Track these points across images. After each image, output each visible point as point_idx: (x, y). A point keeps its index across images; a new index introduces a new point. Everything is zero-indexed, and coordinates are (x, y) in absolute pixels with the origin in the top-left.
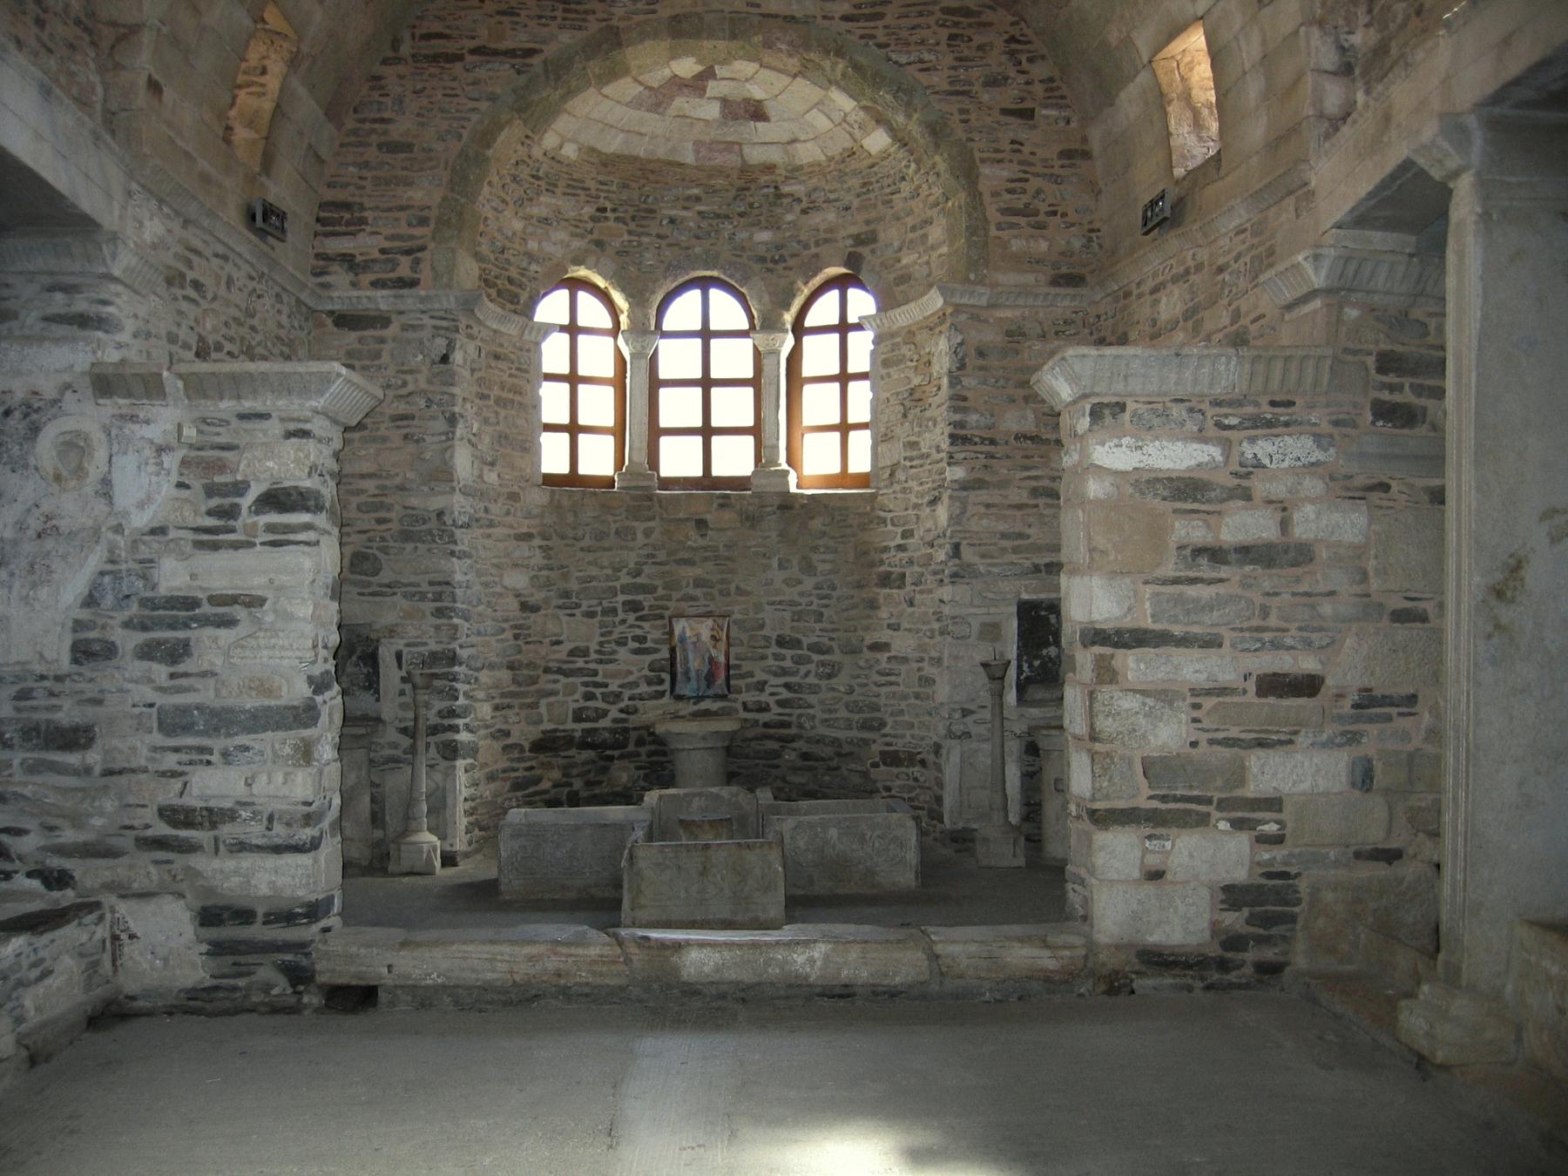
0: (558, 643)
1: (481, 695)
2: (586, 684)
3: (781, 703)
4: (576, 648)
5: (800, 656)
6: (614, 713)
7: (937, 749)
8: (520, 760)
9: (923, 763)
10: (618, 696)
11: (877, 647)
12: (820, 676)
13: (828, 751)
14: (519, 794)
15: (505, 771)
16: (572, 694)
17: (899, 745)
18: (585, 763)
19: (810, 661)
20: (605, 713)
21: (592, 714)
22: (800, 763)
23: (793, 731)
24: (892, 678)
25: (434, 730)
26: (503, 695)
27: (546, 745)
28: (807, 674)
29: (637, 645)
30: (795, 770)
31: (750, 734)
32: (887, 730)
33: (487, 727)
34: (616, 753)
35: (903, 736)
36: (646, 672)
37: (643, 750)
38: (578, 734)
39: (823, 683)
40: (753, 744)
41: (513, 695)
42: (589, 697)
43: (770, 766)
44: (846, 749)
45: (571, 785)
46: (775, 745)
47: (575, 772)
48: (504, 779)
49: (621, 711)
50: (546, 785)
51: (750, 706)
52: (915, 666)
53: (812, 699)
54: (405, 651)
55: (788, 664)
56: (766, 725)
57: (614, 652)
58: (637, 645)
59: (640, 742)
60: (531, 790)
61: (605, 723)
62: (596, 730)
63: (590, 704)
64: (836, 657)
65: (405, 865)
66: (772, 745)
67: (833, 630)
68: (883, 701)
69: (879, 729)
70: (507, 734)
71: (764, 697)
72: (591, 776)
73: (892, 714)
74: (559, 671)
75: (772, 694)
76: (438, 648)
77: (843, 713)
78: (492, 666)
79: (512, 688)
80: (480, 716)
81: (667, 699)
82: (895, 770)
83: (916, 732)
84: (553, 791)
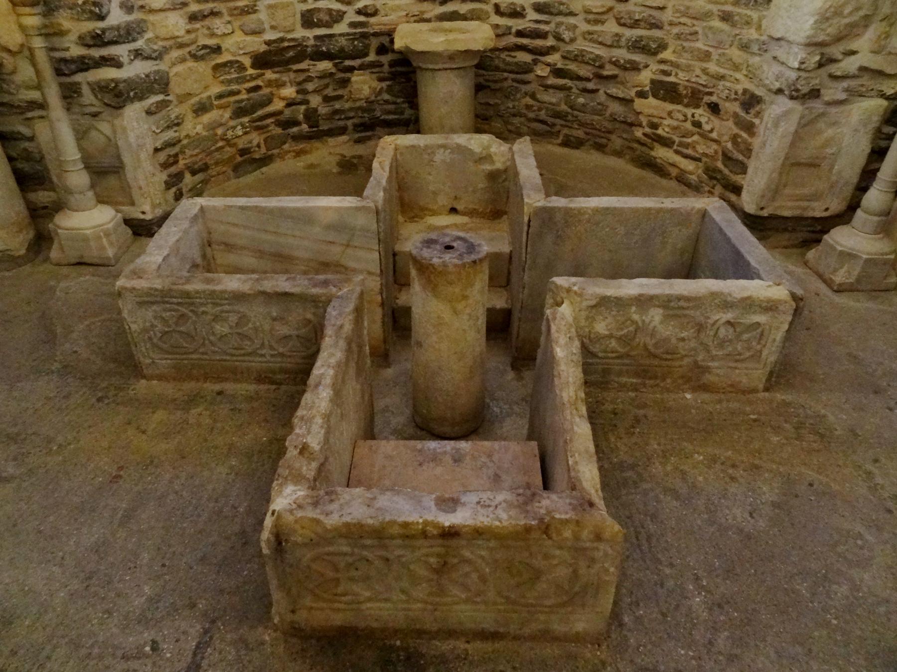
6: (351, 16)
7: (751, 102)
8: (240, 80)
9: (714, 108)
14: (246, 120)
15: (220, 96)
17: (679, 78)
18: (323, 76)
20: (340, 16)
21: (326, 18)
22: (552, 81)
23: (550, 42)
30: (547, 87)
31: (502, 43)
32: (666, 55)
33: (181, 46)
34: (356, 63)
35: (688, 69)
37: (385, 59)
40: (503, 56)
43: (518, 81)
44: (609, 71)
45: (307, 102)
47: (310, 86)
48: (220, 107)
49: (359, 12)
50: (277, 105)
56: (520, 34)
60: (260, 113)
61: (341, 28)
62: (331, 36)
65: (73, 255)
66: (524, 57)
69: (655, 53)
70: (217, 50)
72: (330, 92)
77: (611, 27)
80: (163, 33)
82: (670, 107)
83: (713, 67)
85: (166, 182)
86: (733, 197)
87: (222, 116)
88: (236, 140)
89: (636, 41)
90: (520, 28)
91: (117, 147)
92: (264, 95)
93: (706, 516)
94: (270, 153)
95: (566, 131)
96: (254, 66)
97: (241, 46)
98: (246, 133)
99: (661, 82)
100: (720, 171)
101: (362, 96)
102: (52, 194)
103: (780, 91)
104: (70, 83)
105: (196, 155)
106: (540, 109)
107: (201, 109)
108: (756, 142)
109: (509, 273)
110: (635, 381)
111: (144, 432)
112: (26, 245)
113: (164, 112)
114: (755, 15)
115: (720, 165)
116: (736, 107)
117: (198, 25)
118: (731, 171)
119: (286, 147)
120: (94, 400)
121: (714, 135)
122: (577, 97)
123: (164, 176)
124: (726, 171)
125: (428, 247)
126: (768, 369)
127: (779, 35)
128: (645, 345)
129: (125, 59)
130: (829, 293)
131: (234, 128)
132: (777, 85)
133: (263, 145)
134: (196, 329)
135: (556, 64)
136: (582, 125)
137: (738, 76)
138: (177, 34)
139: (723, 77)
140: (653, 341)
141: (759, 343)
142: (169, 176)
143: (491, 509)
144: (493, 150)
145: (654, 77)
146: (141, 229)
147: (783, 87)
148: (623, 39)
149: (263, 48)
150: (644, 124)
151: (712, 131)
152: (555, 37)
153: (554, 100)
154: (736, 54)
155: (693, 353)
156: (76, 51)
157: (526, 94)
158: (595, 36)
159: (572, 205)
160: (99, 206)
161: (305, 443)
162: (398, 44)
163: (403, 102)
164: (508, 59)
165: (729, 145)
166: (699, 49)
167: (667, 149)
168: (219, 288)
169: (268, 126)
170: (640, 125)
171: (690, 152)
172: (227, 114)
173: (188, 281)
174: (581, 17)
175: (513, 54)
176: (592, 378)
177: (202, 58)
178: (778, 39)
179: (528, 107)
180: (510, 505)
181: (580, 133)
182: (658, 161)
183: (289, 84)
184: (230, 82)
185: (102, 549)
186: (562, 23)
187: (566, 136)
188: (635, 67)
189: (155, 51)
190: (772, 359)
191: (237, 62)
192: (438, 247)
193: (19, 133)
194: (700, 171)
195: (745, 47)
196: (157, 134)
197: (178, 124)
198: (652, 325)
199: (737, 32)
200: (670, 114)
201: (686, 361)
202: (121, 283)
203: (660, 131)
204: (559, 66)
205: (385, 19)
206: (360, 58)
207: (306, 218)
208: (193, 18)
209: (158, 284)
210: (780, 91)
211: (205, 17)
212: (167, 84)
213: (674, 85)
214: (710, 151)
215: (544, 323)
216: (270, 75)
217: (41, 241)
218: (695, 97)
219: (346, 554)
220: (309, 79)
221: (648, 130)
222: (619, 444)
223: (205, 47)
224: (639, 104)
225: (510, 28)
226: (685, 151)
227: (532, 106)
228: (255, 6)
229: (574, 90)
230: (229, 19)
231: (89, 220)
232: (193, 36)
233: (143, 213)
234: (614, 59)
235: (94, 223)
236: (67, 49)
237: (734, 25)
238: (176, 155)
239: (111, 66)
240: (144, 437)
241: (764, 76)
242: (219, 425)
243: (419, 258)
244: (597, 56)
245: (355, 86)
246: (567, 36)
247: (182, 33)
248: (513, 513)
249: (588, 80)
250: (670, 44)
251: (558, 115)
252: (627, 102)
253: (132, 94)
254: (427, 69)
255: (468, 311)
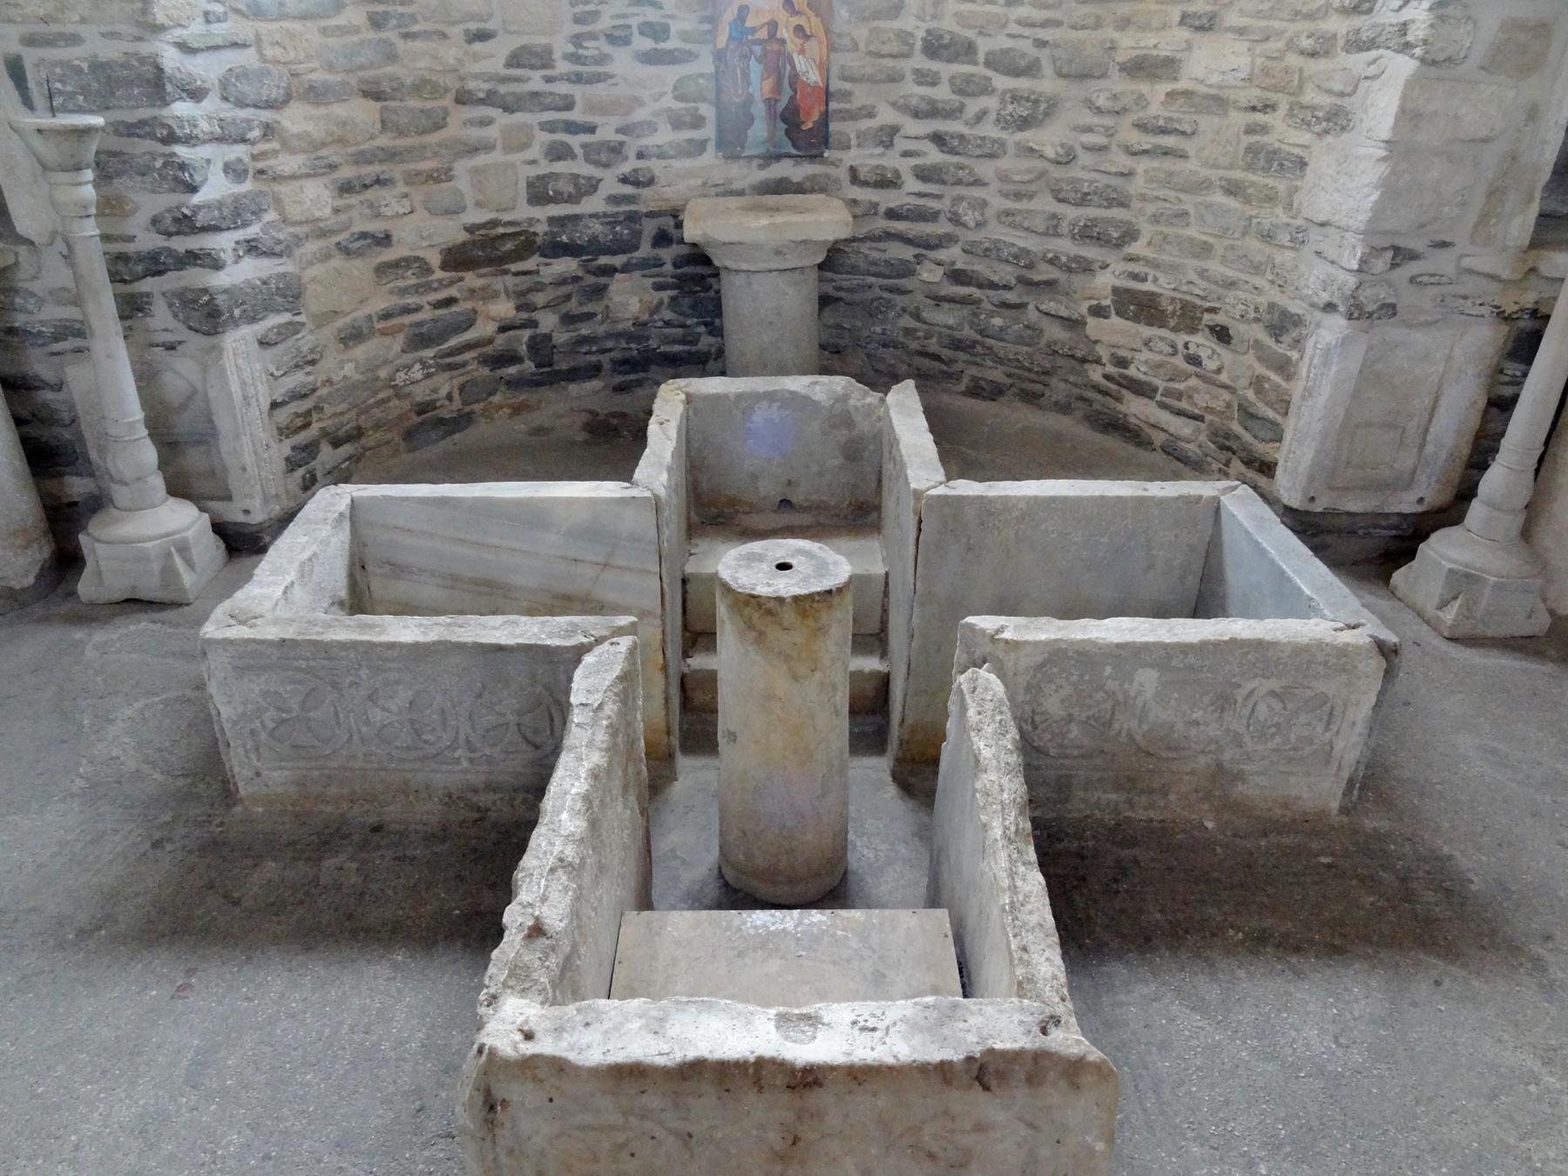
0: (482, 36)
1: (287, 163)
2: (549, 127)
3: (924, 174)
4: (524, 48)
5: (969, 79)
6: (610, 185)
8: (417, 289)
9: (1222, 335)
10: (616, 150)
11: (1141, 67)
12: (1004, 122)
13: (1005, 273)
14: (428, 353)
15: (387, 316)
16: (524, 146)
17: (1160, 285)
18: (562, 281)
19: (986, 89)
20: (593, 186)
23: (941, 228)
24: (1169, 141)
25: (156, 264)
26: (362, 158)
27: (481, 251)
28: (980, 117)
29: (646, 44)
30: (938, 300)
32: (1136, 248)
33: (323, 234)
34: (618, 260)
35: (1174, 268)
36: (669, 102)
37: (667, 254)
38: (542, 228)
39: (1013, 138)
41: (392, 156)
42: (559, 153)
43: (891, 290)
44: (1044, 273)
45: (533, 324)
46: (907, 253)
47: (539, 299)
48: (384, 333)
49: (624, 180)
50: (483, 329)
51: (863, 174)
52: (1239, 119)
53: (985, 169)
54: (30, 57)
55: (942, 93)
56: (892, 214)
57: (602, 59)
58: (646, 44)
59: (662, 239)
60: (454, 342)
61: (594, 204)
62: (575, 218)
63: (560, 167)
64: (1047, 84)
65: (116, 588)
67: (1045, 24)
68: (1137, 186)
69: (1119, 244)
70: (385, 240)
71: (892, 161)
72: (573, 306)
73: (1156, 219)
74: (490, 99)
75: (907, 154)
76: (110, 51)
77: (1045, 204)
78: (315, 94)
79: (384, 141)
81: (710, 157)
82: (1147, 331)
83: (1215, 267)
84: (501, 340)
85: (288, 459)
86: (1262, 481)
87: (389, 348)
88: (411, 388)
89: (1086, 226)
90: (892, 205)
91: (207, 400)
92: (460, 314)
93: (1255, 1043)
94: (468, 409)
95: (973, 371)
96: (445, 266)
97: (425, 234)
98: (428, 376)
99: (1127, 291)
100: (1237, 437)
101: (628, 315)
102: (86, 481)
103: (1330, 307)
104: (133, 296)
105: (342, 413)
106: (928, 336)
107: (352, 337)
108: (1297, 388)
109: (885, 611)
110: (1114, 797)
111: (236, 903)
112: (36, 570)
113: (290, 342)
114: (1281, 186)
115: (1236, 427)
116: (1259, 333)
117: (353, 200)
118: (1255, 437)
119: (496, 399)
120: (147, 845)
121: (1224, 378)
122: (991, 315)
123: (286, 448)
124: (1247, 437)
125: (748, 567)
126: (1346, 774)
127: (1322, 218)
128: (1131, 738)
129: (227, 257)
130: (1438, 642)
131: (408, 367)
132: (1325, 297)
133: (456, 396)
134: (337, 715)
135: (953, 263)
136: (1000, 361)
137: (1257, 281)
138: (318, 214)
139: (1232, 284)
140: (1145, 727)
141: (1327, 728)
142: (294, 448)
143: (878, 1034)
144: (852, 402)
145: (1119, 283)
146: (242, 544)
147: (1335, 300)
148: (1064, 224)
149: (463, 236)
150: (1104, 360)
151: (1219, 371)
152: (950, 220)
153: (951, 322)
154: (1253, 245)
155: (1213, 747)
156: (148, 241)
157: (904, 310)
158: (1018, 219)
159: (992, 493)
160: (172, 501)
161: (537, 918)
162: (691, 232)
163: (698, 324)
164: (875, 255)
165: (1251, 395)
166: (1191, 239)
167: (1146, 401)
168: (384, 638)
169: (464, 364)
170: (1098, 361)
171: (1184, 405)
172: (398, 344)
173: (328, 626)
174: (995, 186)
175: (881, 245)
176: (1042, 791)
177: (359, 253)
178: (1322, 225)
179: (909, 332)
180: (914, 1027)
181: (997, 375)
182: (1133, 420)
183: (503, 295)
184: (403, 291)
185: (151, 1128)
186: (962, 198)
187: (974, 379)
188: (1086, 267)
189: (279, 242)
190: (1352, 757)
191: (417, 259)
192: (764, 566)
193: (37, 378)
194: (1203, 438)
195: (1267, 237)
196: (276, 378)
197: (313, 362)
198: (1139, 702)
199: (1254, 213)
200: (1147, 343)
201: (1202, 761)
202: (210, 630)
203: (1132, 372)
204: (959, 266)
205: (668, 192)
206: (624, 252)
207: (533, 516)
208: (346, 188)
209: (272, 633)
210: (1330, 307)
211: (366, 187)
212: (297, 297)
213: (1153, 297)
214: (1218, 405)
215: (953, 697)
216: (471, 279)
217: (66, 561)
218: (1188, 317)
219: (613, 1128)
220: (538, 287)
221: (1111, 369)
222: (1092, 912)
223: (364, 235)
224: (1093, 326)
225: (875, 205)
226: (1176, 404)
227: (915, 330)
228: (450, 169)
229: (986, 305)
230: (406, 190)
231: (150, 527)
232: (343, 217)
233: (247, 512)
234: (1050, 255)
235: (162, 530)
236: (131, 239)
237: (1247, 201)
238: (309, 413)
239: (202, 266)
240: (237, 911)
241: (1302, 282)
242: (374, 887)
243: (734, 585)
244: (1023, 250)
245: (616, 299)
246: (969, 218)
247: (328, 211)
248: (917, 1040)
249: (1007, 287)
250: (1143, 231)
251: (958, 345)
252: (1074, 324)
253: (237, 312)
254: (737, 271)
255: (818, 676)
